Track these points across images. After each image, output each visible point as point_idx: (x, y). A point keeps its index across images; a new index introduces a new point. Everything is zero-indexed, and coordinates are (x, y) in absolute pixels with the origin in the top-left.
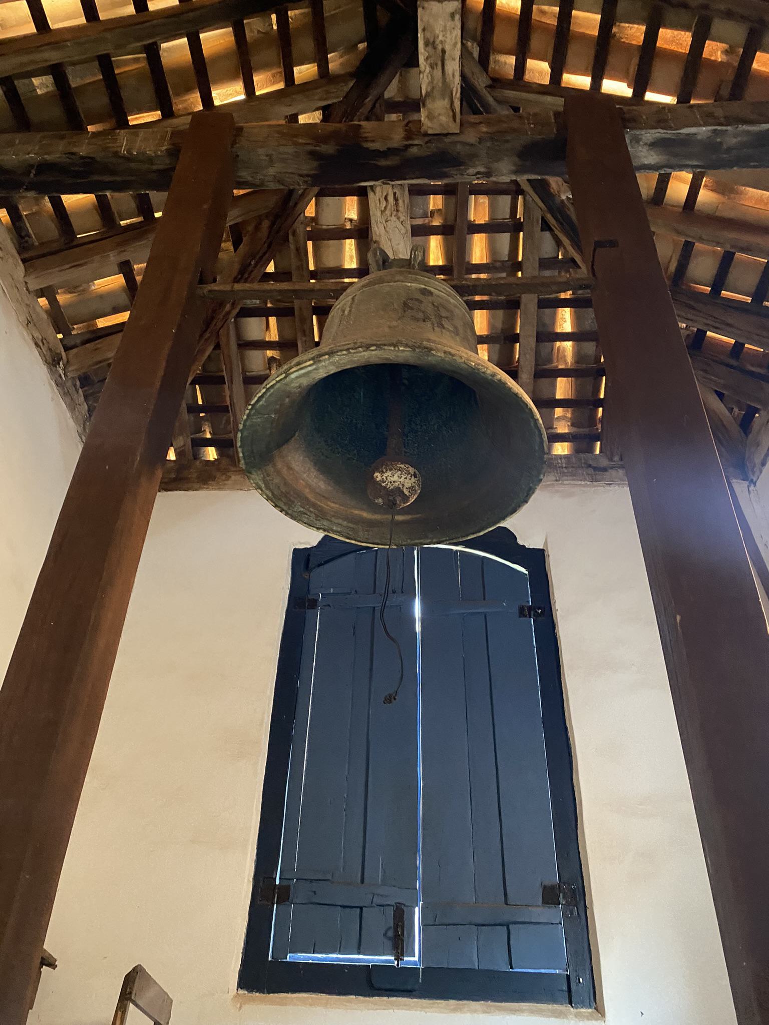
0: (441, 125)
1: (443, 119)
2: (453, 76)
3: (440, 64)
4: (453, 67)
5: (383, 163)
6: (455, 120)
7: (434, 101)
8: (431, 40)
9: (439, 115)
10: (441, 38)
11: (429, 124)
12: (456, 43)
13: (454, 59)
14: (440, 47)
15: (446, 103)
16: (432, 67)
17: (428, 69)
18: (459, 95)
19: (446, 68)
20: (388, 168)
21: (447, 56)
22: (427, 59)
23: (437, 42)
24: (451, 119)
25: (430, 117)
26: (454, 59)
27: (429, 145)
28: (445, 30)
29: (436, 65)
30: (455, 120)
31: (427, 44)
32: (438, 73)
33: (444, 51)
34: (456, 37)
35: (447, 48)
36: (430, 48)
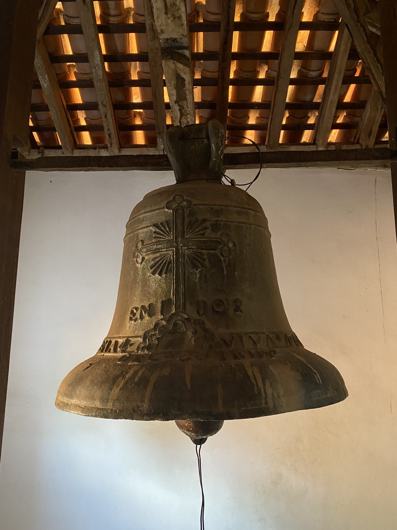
3: (169, 6)
8: (176, 19)
10: (169, 21)
12: (158, 18)
14: (169, 16)
16: (174, 4)
19: (163, 4)
22: (179, 9)
23: (171, 19)
26: (158, 9)
28: (167, 25)
29: (171, 5)
31: (180, 18)
33: (166, 13)
34: (158, 21)
35: (164, 16)
36: (177, 15)
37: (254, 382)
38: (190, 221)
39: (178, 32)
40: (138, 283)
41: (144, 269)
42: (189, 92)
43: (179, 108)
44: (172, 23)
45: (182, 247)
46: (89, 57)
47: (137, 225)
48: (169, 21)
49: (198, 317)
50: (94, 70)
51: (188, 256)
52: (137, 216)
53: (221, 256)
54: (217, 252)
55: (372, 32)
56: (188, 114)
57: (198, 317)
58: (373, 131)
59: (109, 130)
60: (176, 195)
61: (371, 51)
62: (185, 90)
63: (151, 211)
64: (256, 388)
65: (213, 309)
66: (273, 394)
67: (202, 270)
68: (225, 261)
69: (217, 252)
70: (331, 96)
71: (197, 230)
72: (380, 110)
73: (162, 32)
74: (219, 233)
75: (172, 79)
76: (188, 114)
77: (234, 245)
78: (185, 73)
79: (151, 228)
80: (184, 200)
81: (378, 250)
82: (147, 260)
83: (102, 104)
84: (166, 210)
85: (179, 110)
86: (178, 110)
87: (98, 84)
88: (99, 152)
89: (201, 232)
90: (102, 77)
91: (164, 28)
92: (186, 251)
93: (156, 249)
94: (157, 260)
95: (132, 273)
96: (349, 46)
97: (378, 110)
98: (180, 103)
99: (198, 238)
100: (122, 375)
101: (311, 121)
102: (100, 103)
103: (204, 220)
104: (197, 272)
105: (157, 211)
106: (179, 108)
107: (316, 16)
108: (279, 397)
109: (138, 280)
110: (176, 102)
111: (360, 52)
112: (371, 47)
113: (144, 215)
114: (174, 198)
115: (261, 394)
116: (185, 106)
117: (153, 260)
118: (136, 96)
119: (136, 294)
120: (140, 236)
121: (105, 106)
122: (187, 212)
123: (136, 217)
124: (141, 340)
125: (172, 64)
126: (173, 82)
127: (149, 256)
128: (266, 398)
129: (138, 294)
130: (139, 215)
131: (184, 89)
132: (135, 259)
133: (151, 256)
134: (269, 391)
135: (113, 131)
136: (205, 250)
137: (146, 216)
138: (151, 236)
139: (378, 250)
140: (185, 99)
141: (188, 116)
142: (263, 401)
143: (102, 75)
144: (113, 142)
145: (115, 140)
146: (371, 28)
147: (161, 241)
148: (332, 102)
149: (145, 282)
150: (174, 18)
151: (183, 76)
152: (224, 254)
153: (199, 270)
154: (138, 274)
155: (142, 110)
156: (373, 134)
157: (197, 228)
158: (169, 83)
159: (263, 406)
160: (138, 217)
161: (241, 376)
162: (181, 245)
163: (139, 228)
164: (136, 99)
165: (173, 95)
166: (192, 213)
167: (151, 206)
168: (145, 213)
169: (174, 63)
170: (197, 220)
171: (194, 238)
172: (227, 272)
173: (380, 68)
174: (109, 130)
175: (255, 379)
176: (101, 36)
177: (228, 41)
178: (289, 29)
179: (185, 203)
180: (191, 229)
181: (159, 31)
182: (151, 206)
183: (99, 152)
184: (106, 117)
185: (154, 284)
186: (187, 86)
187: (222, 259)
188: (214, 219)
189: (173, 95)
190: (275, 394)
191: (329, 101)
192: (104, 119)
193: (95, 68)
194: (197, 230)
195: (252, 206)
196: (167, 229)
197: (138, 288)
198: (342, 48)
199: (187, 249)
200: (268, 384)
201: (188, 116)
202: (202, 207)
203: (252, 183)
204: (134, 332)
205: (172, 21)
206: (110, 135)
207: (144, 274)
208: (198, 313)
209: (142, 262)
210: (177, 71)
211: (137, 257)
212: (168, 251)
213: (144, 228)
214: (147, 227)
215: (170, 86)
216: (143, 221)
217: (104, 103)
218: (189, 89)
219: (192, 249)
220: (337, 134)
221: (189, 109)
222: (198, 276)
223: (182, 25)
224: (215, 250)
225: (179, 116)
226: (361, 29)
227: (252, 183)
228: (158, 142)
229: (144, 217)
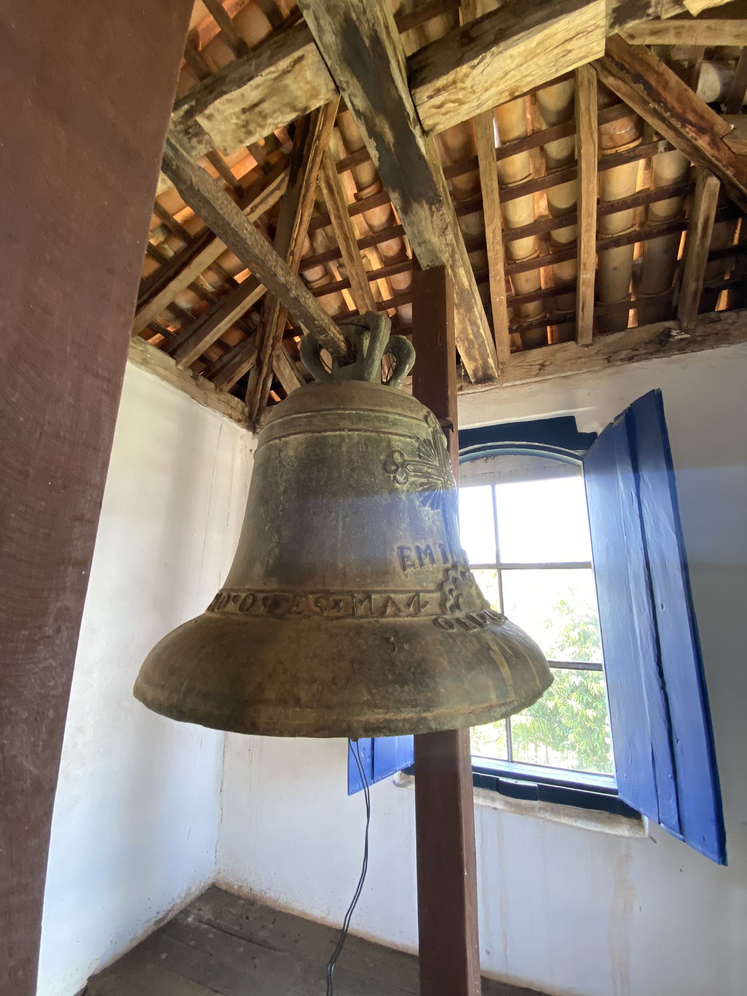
0: (316, 74)
1: (309, 74)
2: (258, 86)
3: (257, 110)
4: (251, 92)
5: (389, 136)
6: (301, 59)
7: (296, 98)
8: (244, 130)
9: (307, 83)
11: (323, 90)
13: (243, 95)
14: (243, 117)
15: (289, 80)
16: (265, 117)
17: (270, 121)
18: (272, 69)
19: (256, 100)
20: (393, 127)
21: (245, 105)
22: (262, 127)
23: (240, 123)
24: (304, 62)
25: (315, 95)
26: (243, 95)
27: (344, 85)
28: (226, 120)
29: (260, 113)
30: (301, 59)
31: (250, 133)
32: (266, 107)
33: (244, 111)
34: (223, 104)
35: (238, 109)
36: (252, 127)
39: (225, 141)
44: (233, 127)
48: (235, 121)
73: (209, 118)
79: (413, 440)
82: (413, 483)
91: (219, 117)
101: (170, 329)
109: (401, 507)
113: (396, 417)
117: (422, 484)
132: (392, 476)
148: (219, 329)
185: (427, 519)
205: (236, 124)
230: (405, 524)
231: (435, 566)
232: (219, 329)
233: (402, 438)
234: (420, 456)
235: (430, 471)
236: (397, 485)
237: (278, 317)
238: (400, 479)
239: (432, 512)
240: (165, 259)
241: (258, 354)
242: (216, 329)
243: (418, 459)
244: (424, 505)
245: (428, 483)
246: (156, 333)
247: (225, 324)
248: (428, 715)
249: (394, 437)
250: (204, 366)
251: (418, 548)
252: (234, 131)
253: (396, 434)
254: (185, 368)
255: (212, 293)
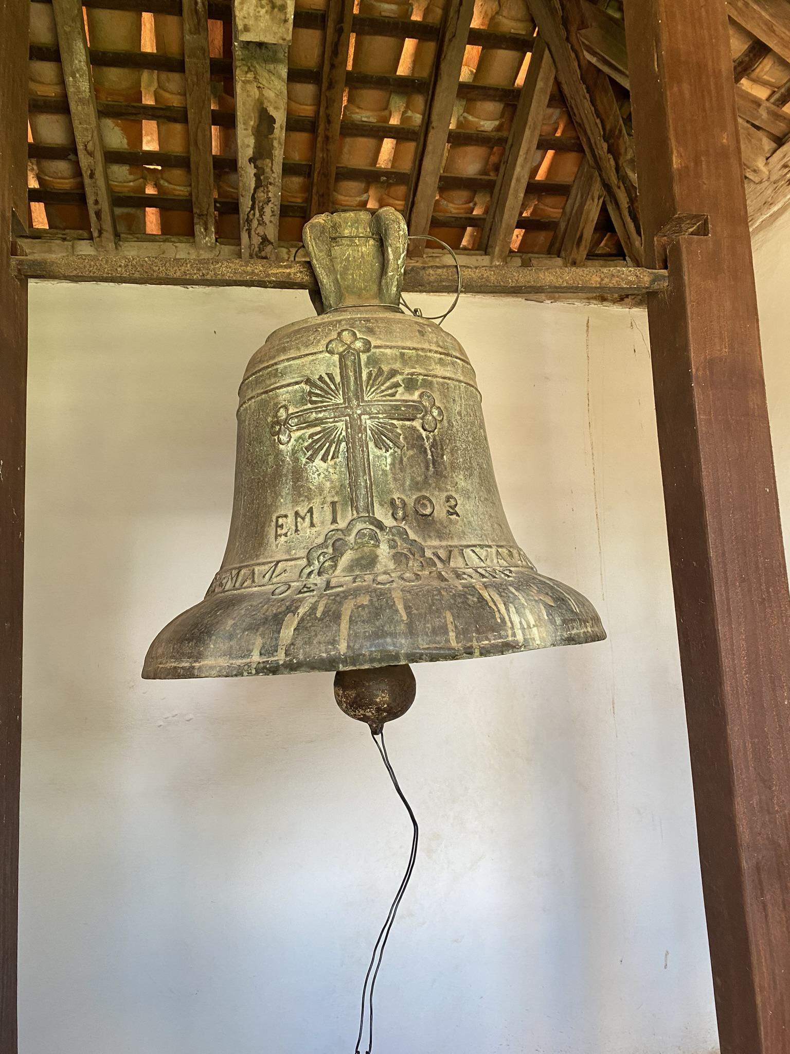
8: (276, 10)
10: (263, 11)
28: (257, 18)
37: (494, 607)
38: (370, 375)
39: (275, 33)
40: (286, 475)
41: (294, 452)
42: (280, 143)
43: (255, 171)
44: (267, 17)
45: (360, 415)
46: (61, 51)
47: (273, 380)
48: (263, 11)
49: (395, 524)
50: (71, 79)
51: (372, 430)
52: (273, 365)
53: (422, 430)
54: (417, 424)
55: (590, 62)
56: (271, 184)
57: (395, 524)
58: (585, 236)
59: (96, 202)
60: (343, 331)
61: (587, 96)
62: (272, 140)
63: (300, 357)
64: (497, 615)
65: (416, 512)
66: (521, 623)
67: (395, 452)
68: (428, 438)
69: (417, 424)
70: (518, 169)
71: (383, 388)
72: (596, 200)
73: (246, 29)
74: (417, 394)
75: (250, 118)
76: (271, 184)
77: (441, 413)
78: (276, 108)
79: (303, 385)
80: (356, 339)
81: (592, 444)
82: (300, 437)
83: (86, 149)
84: (327, 354)
85: (255, 175)
86: (252, 175)
87: (80, 108)
88: (73, 246)
89: (390, 391)
90: (88, 94)
91: (251, 22)
92: (368, 422)
93: (317, 419)
94: (315, 438)
95: (271, 459)
96: (552, 81)
97: (593, 200)
98: (259, 163)
99: (387, 401)
100: (292, 609)
102: (80, 147)
103: (393, 373)
104: (388, 454)
105: (311, 358)
106: (255, 171)
107: (492, 21)
108: (529, 627)
109: (285, 471)
110: (250, 160)
111: (568, 95)
112: (587, 88)
113: (287, 364)
114: (339, 334)
115: (506, 623)
116: (268, 170)
117: (311, 436)
118: (149, 138)
119: (284, 494)
120: (280, 398)
121: (91, 154)
122: (364, 357)
123: (268, 367)
124: (305, 561)
125: (256, 90)
126: (252, 123)
127: (303, 431)
128: (512, 628)
129: (288, 494)
130: (276, 364)
131: (271, 136)
132: (276, 438)
133: (305, 431)
134: (516, 619)
135: (105, 205)
136: (398, 419)
137: (290, 366)
138: (302, 398)
139: (592, 444)
140: (270, 156)
141: (270, 187)
142: (510, 632)
143: (87, 90)
144: (104, 227)
145: (107, 225)
146: (588, 56)
147: (325, 406)
148: (518, 180)
149: (298, 474)
150: (273, 7)
151: (272, 112)
152: (427, 427)
153: (391, 451)
154: (283, 461)
155: (160, 168)
156: (583, 243)
157: (382, 385)
158: (244, 124)
159: (510, 639)
160: (275, 367)
161: (475, 599)
162: (359, 412)
163: (278, 385)
164: (148, 142)
165: (248, 146)
166: (372, 361)
167: (299, 349)
168: (288, 360)
169: (259, 87)
170: (380, 371)
171: (379, 401)
172: (432, 456)
173: (600, 126)
174: (96, 202)
175: (496, 605)
176: (84, 9)
177: (337, 50)
178: (450, 40)
179: (359, 345)
180: (372, 386)
181: (240, 27)
182: (299, 349)
183: (73, 246)
184: (92, 176)
186: (277, 131)
187: (424, 434)
188: (407, 371)
189: (248, 146)
190: (524, 623)
191: (515, 177)
192: (87, 181)
193: (74, 76)
194: (383, 388)
195: (453, 353)
196: (333, 387)
197: (287, 484)
198: (540, 84)
199: (371, 418)
200: (512, 609)
201: (270, 187)
202: (388, 351)
203: (445, 316)
204: (288, 552)
205: (267, 12)
206: (98, 214)
207: (296, 460)
208: (396, 519)
209: (288, 442)
210: (262, 103)
211: (278, 433)
212: (337, 422)
213: (289, 385)
214: (297, 383)
215: (246, 129)
216: (283, 374)
217: (90, 147)
218: (280, 138)
219: (378, 418)
220: (520, 238)
221: (275, 175)
222: (389, 460)
223: (286, 21)
224: (413, 420)
225: (253, 185)
226: (573, 55)
227: (445, 316)
228: (197, 233)
229: (285, 367)
230: (286, 489)
231: (314, 529)
232: (518, 180)
233: (290, 388)
234: (312, 402)
235: (320, 415)
236: (281, 446)
237: (593, 102)
238: (284, 438)
239: (324, 465)
240: (414, 133)
241: (600, 175)
242: (514, 181)
243: (309, 406)
244: (311, 459)
245: (324, 430)
246: (465, 229)
247: (523, 167)
248: (197, 665)
249: (281, 390)
250: (542, 237)
251: (297, 514)
252: (272, 19)
253: (282, 387)
254: (505, 260)
255: (499, 129)
